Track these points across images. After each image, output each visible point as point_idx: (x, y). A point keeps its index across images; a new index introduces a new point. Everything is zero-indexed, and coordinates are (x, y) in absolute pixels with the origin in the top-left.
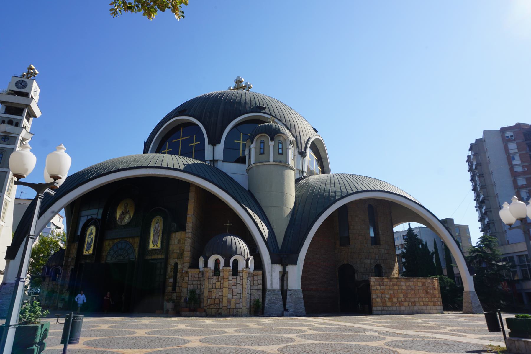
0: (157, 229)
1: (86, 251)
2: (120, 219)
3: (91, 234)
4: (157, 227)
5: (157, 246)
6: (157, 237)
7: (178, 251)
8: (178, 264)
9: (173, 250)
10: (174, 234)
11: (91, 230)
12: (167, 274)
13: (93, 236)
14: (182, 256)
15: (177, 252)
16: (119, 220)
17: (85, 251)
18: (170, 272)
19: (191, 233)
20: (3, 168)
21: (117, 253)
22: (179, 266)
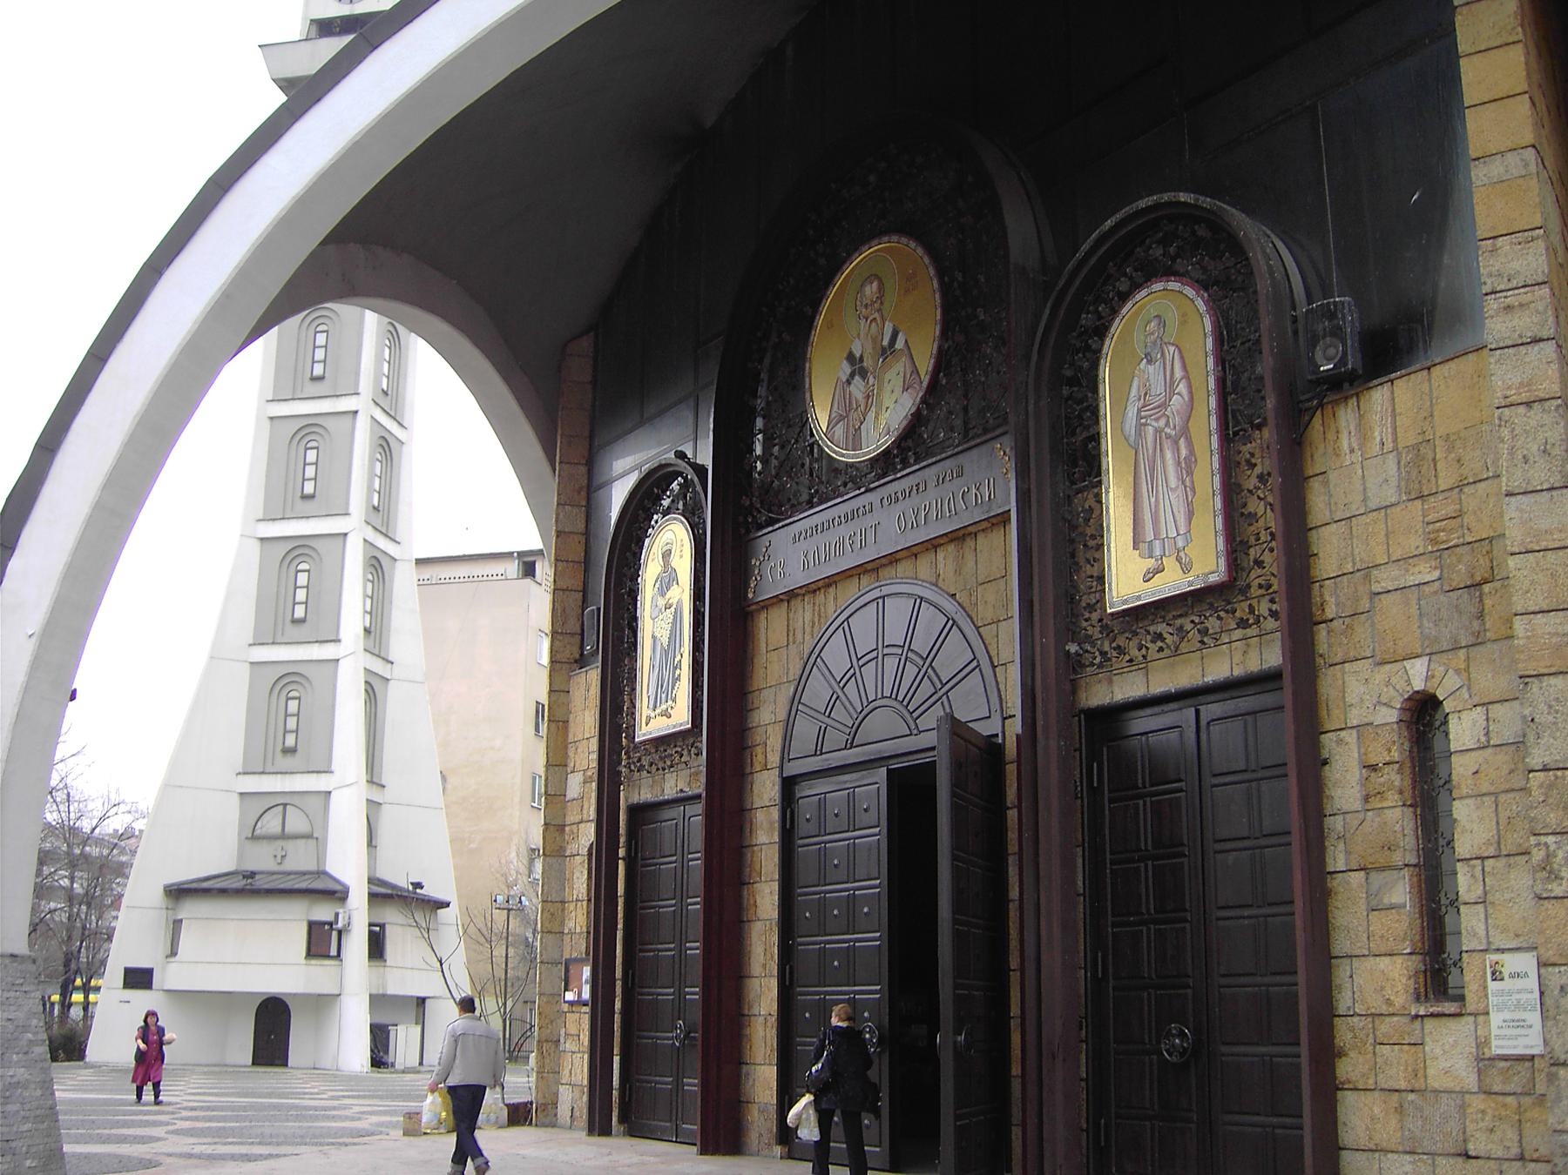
0: (1164, 405)
1: (655, 707)
2: (841, 418)
3: (667, 580)
4: (1158, 388)
5: (1186, 568)
6: (1173, 482)
7: (1425, 572)
8: (1448, 706)
9: (1367, 578)
10: (1346, 416)
11: (667, 555)
12: (1335, 824)
13: (682, 593)
14: (1481, 616)
15: (1412, 580)
16: (839, 431)
17: (644, 708)
18: (1367, 798)
19: (1549, 349)
20: (337, 396)
21: (851, 689)
22: (1462, 730)
